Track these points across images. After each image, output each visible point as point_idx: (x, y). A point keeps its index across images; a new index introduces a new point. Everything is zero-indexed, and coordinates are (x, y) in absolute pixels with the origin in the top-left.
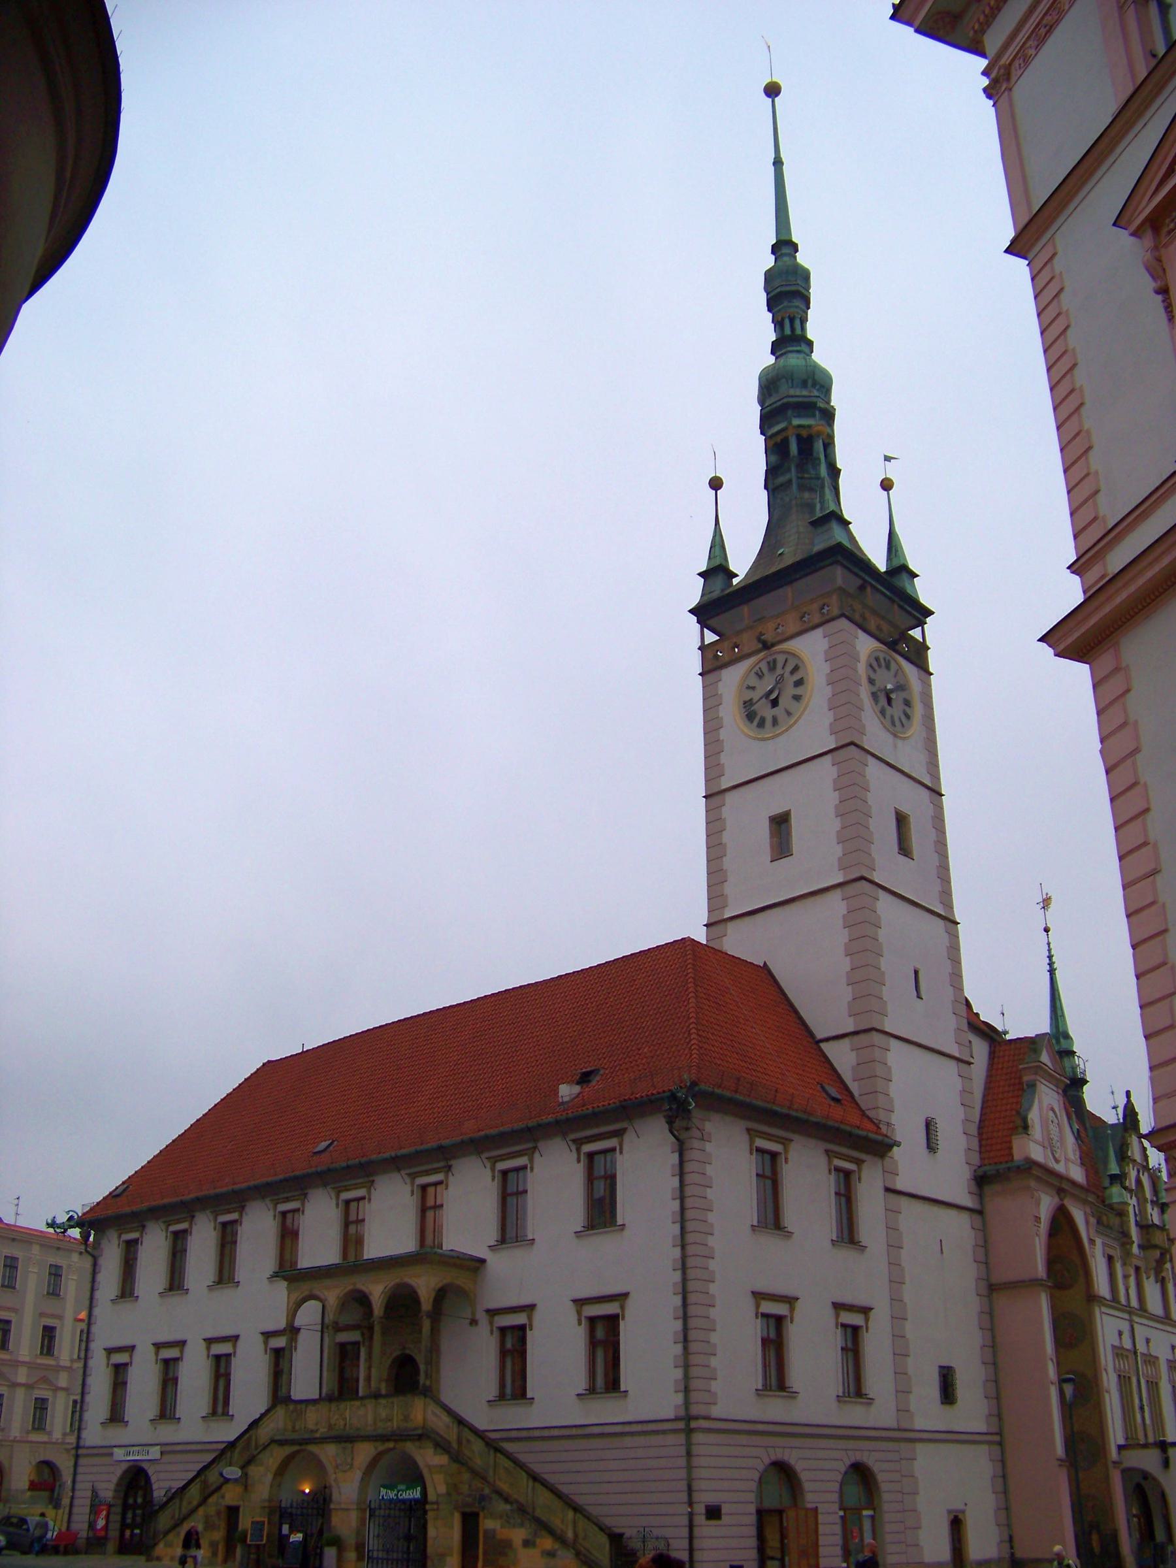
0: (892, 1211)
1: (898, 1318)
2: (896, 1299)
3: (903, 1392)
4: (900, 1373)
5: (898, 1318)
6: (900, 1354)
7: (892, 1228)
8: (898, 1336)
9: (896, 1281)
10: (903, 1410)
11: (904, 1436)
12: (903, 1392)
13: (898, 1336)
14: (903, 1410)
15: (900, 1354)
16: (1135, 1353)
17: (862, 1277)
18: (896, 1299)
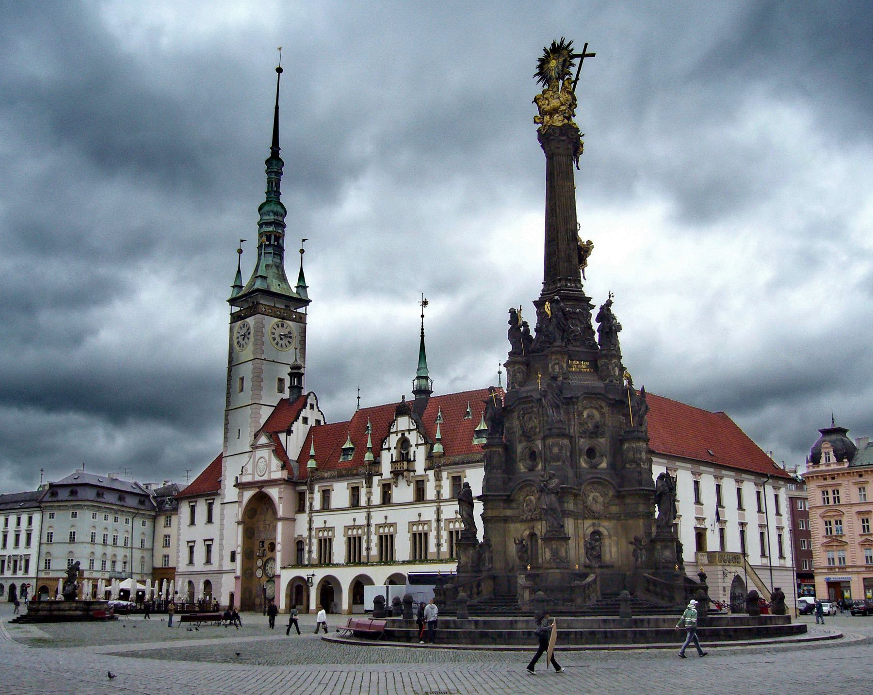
0: (222, 510)
1: (221, 540)
2: (222, 535)
3: (221, 560)
4: (221, 556)
5: (221, 540)
6: (221, 550)
7: (222, 515)
8: (221, 545)
9: (222, 529)
10: (221, 565)
11: (220, 572)
12: (221, 560)
13: (221, 545)
14: (221, 565)
15: (221, 550)
16: (369, 525)
17: (212, 531)
18: (222, 535)
